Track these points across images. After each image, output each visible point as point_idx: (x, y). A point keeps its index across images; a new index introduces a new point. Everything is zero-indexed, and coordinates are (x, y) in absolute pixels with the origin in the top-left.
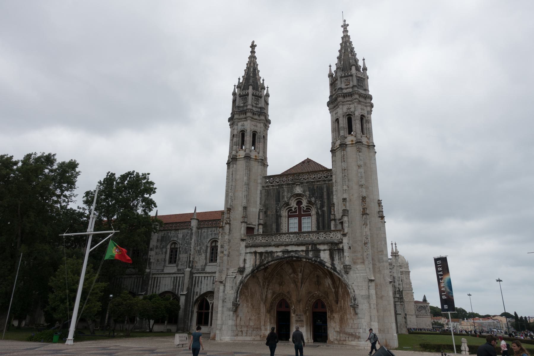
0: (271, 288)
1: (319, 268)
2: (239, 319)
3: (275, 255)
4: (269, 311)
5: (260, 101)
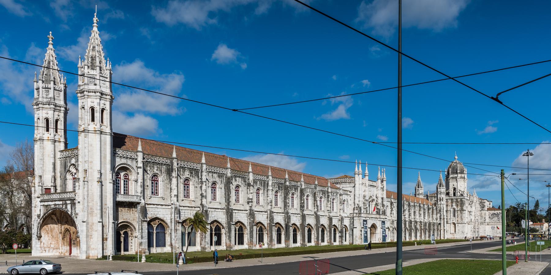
3: (51, 207)
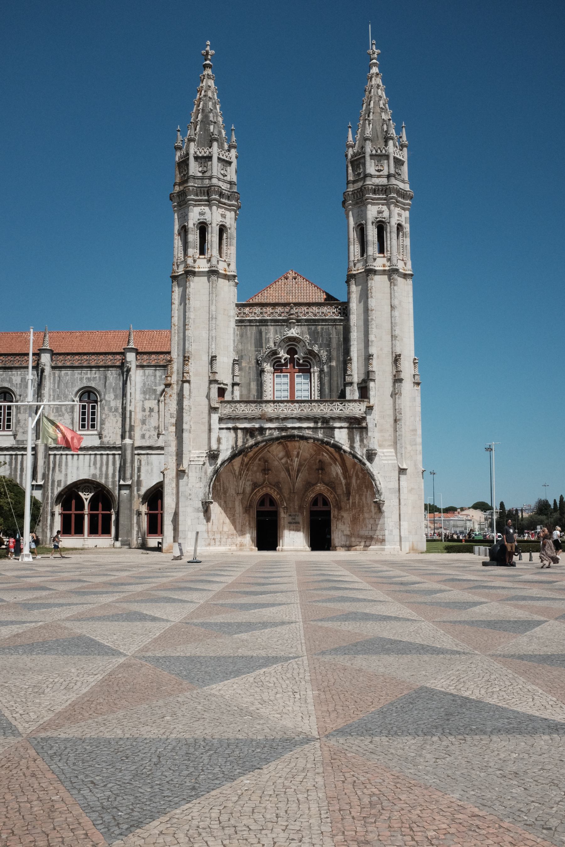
0: (250, 478)
4: (247, 510)
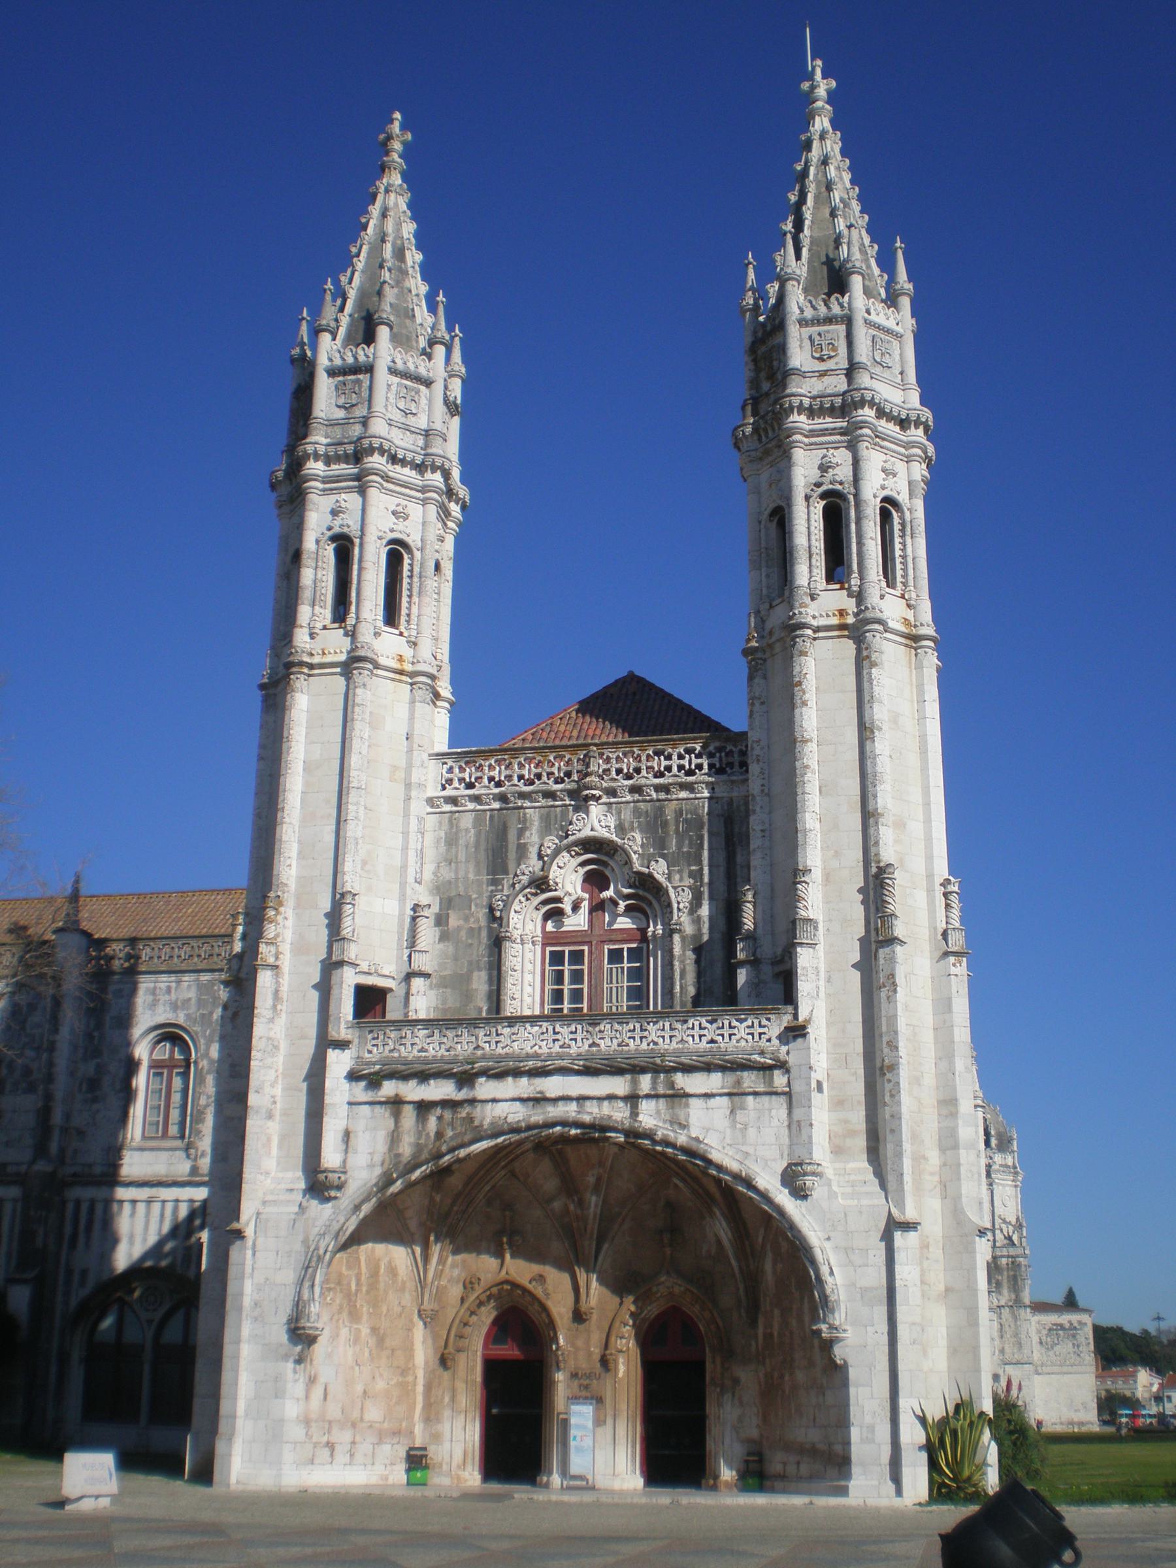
1: (679, 1171)
2: (317, 1392)
5: (424, 402)
